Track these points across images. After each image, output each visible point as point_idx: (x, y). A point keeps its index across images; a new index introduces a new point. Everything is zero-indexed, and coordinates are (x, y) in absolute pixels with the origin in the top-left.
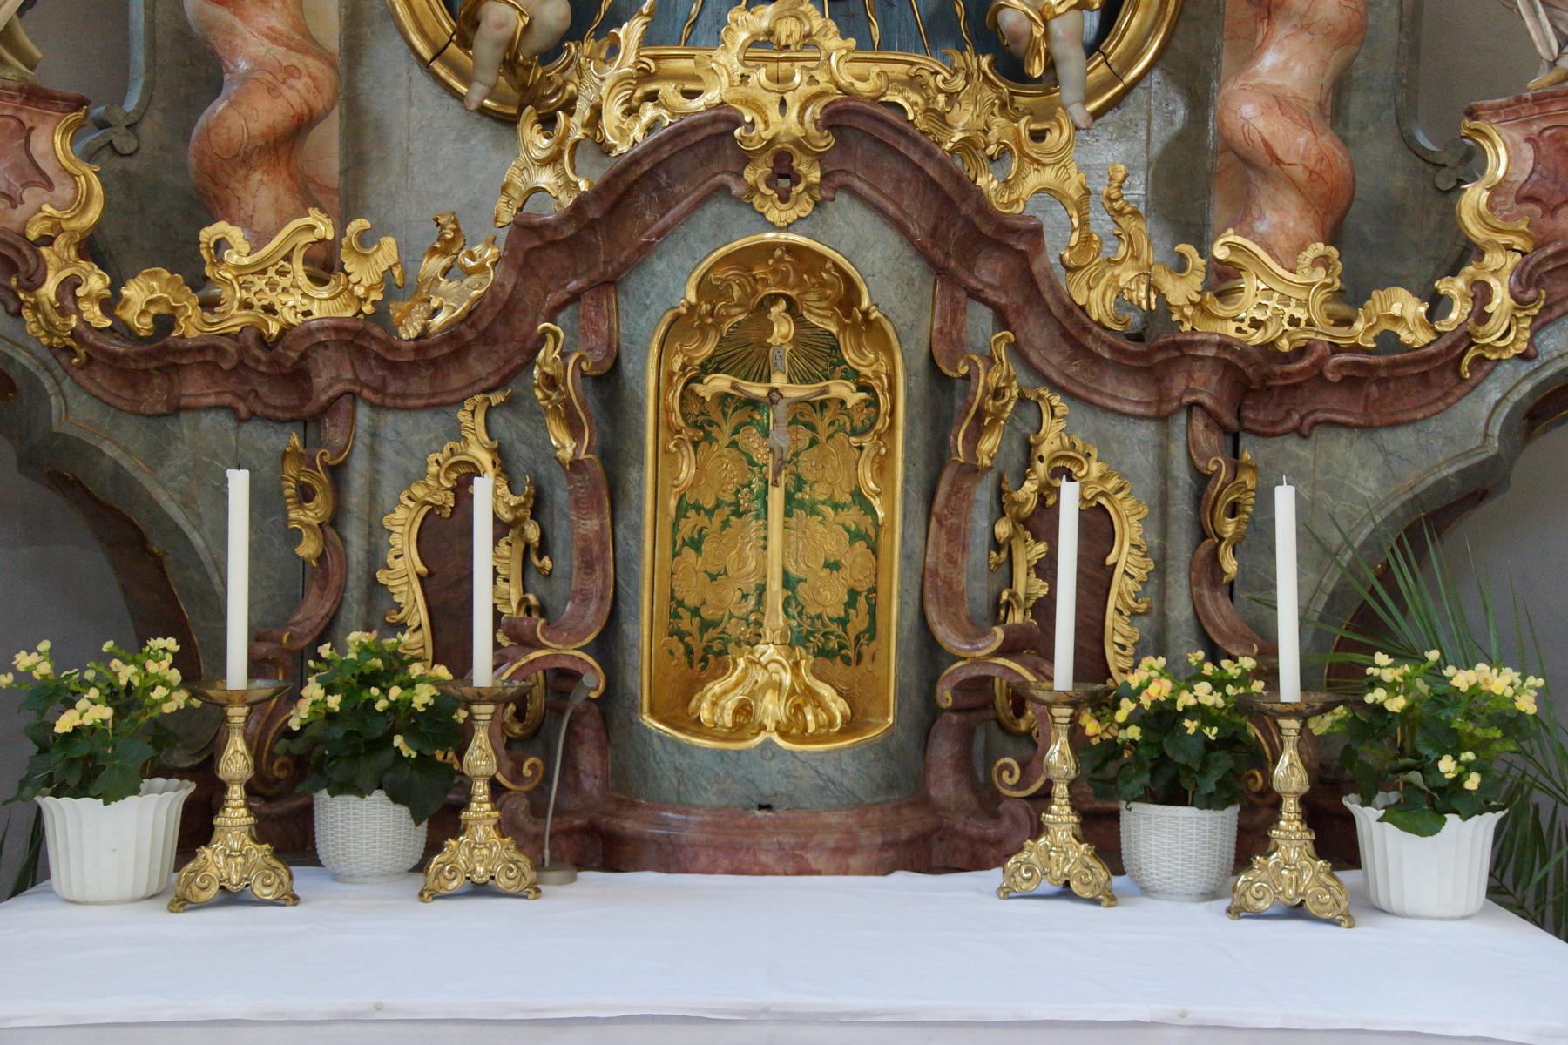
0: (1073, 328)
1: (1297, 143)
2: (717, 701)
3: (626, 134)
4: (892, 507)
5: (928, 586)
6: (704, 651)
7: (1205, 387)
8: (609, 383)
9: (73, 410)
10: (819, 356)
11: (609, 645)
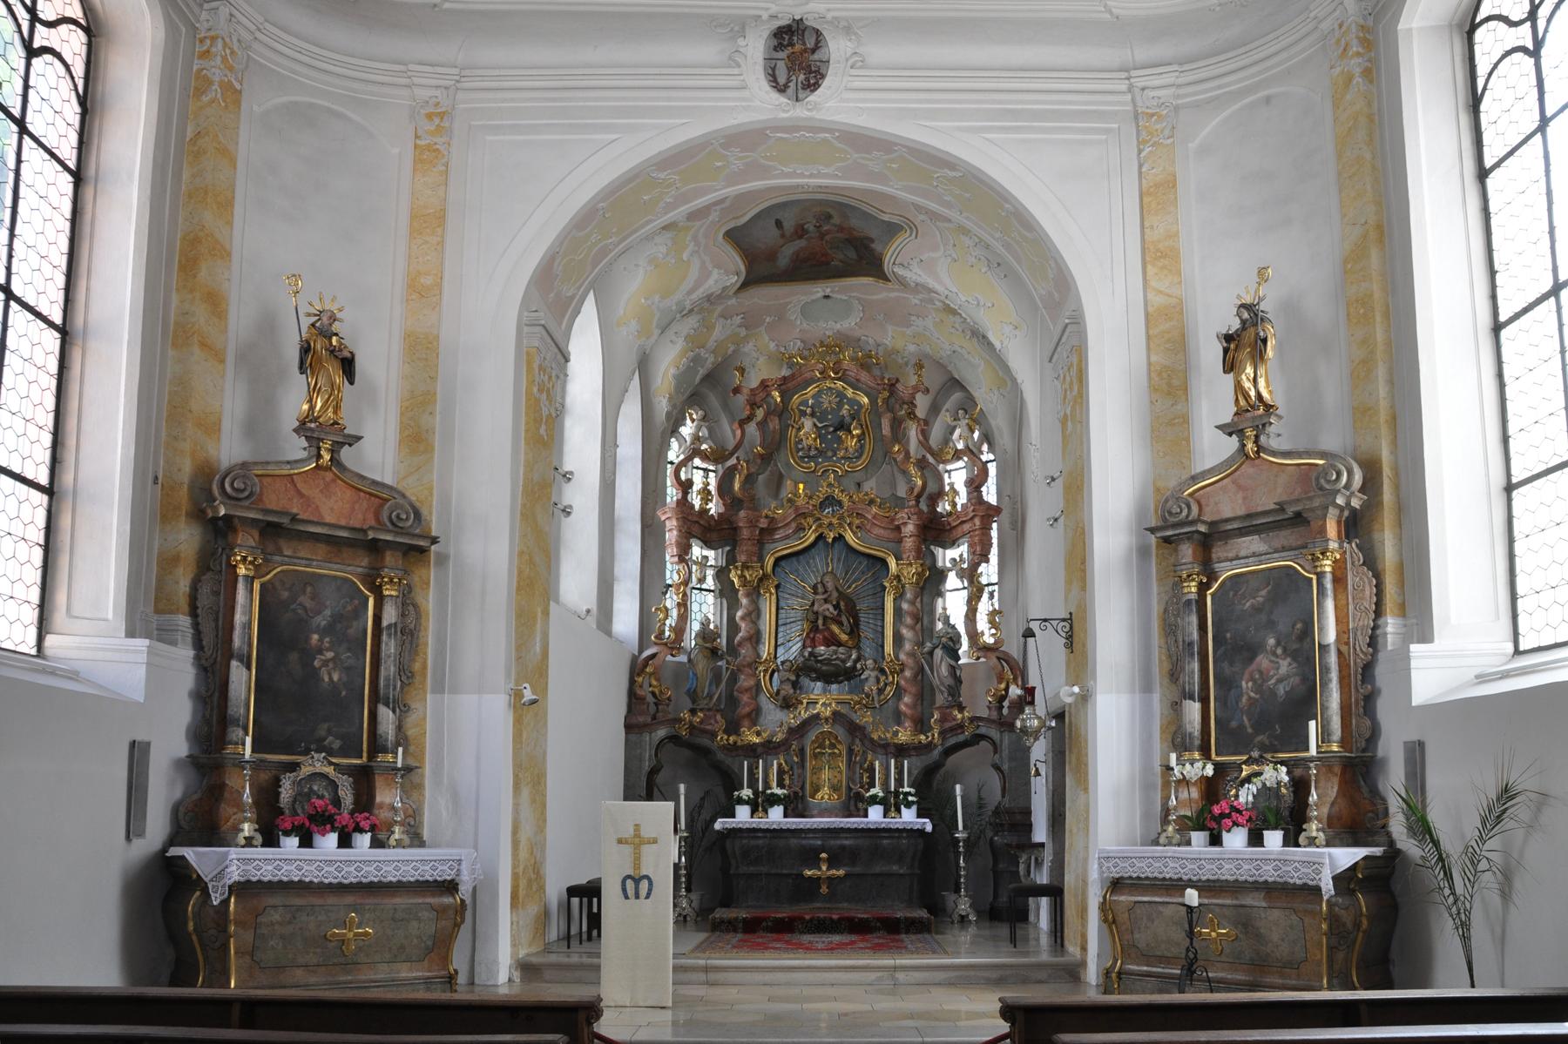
0: (872, 740)
1: (909, 712)
2: (819, 795)
3: (805, 715)
4: (843, 768)
5: (849, 779)
6: (816, 789)
7: (892, 749)
8: (802, 751)
9: (720, 756)
10: (833, 746)
11: (803, 788)
